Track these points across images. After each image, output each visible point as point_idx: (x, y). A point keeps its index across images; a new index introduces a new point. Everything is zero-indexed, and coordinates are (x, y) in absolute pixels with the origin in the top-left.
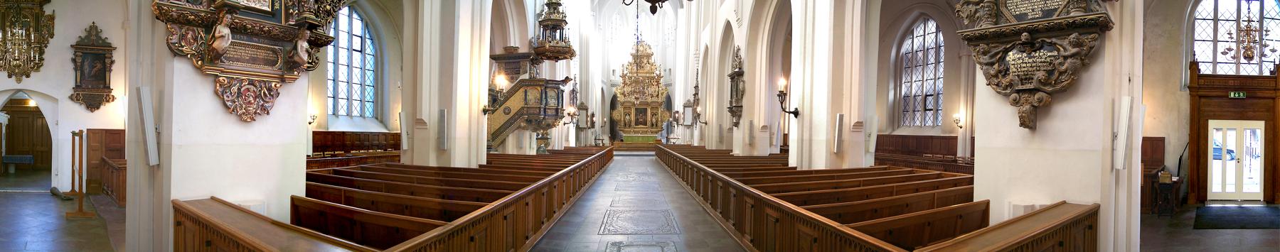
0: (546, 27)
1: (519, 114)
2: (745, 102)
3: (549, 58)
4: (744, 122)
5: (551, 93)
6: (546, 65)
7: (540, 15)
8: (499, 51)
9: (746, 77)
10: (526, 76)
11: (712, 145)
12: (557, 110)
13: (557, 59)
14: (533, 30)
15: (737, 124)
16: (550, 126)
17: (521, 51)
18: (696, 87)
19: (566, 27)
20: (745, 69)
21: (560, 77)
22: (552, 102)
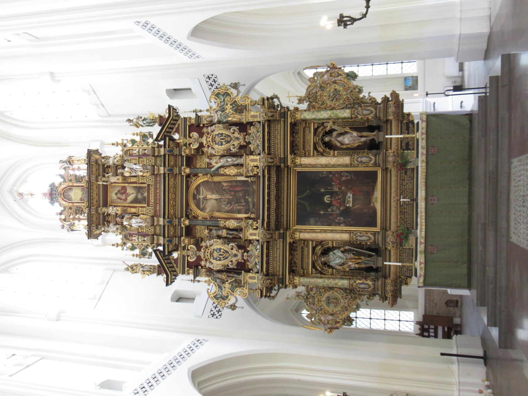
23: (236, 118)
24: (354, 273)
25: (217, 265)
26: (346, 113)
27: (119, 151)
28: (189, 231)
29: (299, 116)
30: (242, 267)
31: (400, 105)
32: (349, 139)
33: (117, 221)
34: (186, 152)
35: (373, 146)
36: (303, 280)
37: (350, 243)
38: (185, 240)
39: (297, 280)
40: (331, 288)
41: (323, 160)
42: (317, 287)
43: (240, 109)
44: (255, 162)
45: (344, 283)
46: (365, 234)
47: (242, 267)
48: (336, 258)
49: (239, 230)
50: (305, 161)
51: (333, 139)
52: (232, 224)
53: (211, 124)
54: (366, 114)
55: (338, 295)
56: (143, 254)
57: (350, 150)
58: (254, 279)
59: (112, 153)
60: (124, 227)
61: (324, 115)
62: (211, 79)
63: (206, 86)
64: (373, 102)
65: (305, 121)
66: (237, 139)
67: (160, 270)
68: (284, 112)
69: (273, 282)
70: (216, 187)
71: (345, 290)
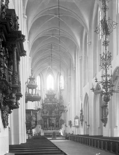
2: (108, 117)
4: (108, 125)
9: (108, 108)
15: (105, 126)
18: (82, 111)
25: (44, 110)
26: (60, 124)
27: (56, 98)
28: (47, 107)
30: (44, 113)
32: (57, 124)
33: (48, 98)
35: (56, 126)
36: (43, 120)
38: (46, 106)
39: (43, 119)
40: (42, 122)
42: (42, 121)
46: (48, 126)
47: (44, 113)
48: (45, 123)
49: (48, 113)
51: (57, 123)
52: (48, 112)
55: (42, 123)
56: (44, 101)
57: (56, 124)
58: (43, 115)
60: (47, 99)
61: (60, 122)
65: (59, 119)
67: (43, 103)
68: (60, 117)
69: (42, 117)
70: (52, 110)
71: (42, 124)
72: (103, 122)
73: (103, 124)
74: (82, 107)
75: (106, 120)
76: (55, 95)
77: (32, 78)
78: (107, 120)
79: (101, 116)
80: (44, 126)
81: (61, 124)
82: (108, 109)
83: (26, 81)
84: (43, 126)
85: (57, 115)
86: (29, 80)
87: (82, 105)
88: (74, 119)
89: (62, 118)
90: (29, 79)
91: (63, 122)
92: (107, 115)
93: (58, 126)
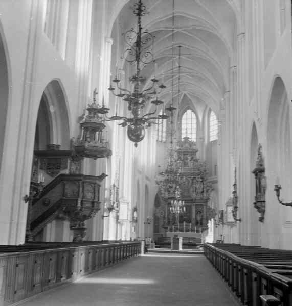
0: (86, 129)
1: (58, 205)
3: (88, 156)
5: (88, 188)
6: (86, 161)
7: (81, 118)
8: (42, 148)
10: (67, 172)
11: (247, 242)
12: (93, 203)
13: (95, 157)
14: (74, 131)
16: (85, 217)
17: (61, 149)
19: (103, 130)
20: (266, 165)
21: (98, 174)
22: (89, 196)
23: (205, 190)
24: (169, 219)
27: (198, 158)
29: (205, 207)
31: (205, 229)
32: (199, 218)
33: (180, 158)
34: (197, 177)
35: (197, 223)
37: (175, 218)
40: (165, 213)
41: (194, 212)
43: (207, 191)
44: (194, 196)
45: (166, 216)
46: (178, 221)
50: (194, 208)
53: (203, 184)
54: (204, 222)
57: (196, 218)
59: (198, 155)
62: (216, 182)
63: (215, 179)
64: (207, 223)
66: (200, 191)
71: (165, 215)
72: (260, 212)
73: (259, 215)
74: (235, 176)
75: (263, 204)
76: (197, 151)
77: (93, 109)
78: (264, 206)
79: (255, 195)
80: (169, 222)
81: (207, 220)
82: (265, 178)
83: (80, 115)
84: (166, 219)
85: (200, 196)
86: (87, 112)
87: (235, 171)
88: (225, 206)
89: (211, 205)
90: (88, 109)
91: (211, 214)
92: (265, 193)
93: (202, 224)
